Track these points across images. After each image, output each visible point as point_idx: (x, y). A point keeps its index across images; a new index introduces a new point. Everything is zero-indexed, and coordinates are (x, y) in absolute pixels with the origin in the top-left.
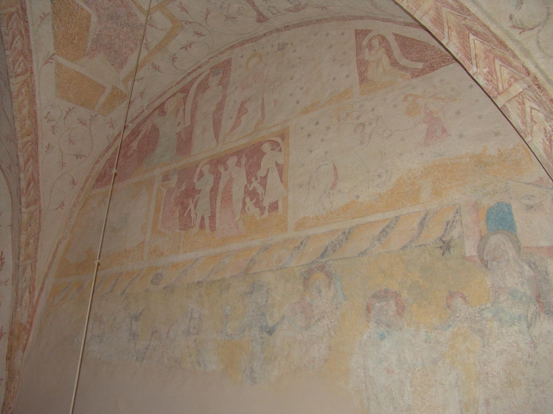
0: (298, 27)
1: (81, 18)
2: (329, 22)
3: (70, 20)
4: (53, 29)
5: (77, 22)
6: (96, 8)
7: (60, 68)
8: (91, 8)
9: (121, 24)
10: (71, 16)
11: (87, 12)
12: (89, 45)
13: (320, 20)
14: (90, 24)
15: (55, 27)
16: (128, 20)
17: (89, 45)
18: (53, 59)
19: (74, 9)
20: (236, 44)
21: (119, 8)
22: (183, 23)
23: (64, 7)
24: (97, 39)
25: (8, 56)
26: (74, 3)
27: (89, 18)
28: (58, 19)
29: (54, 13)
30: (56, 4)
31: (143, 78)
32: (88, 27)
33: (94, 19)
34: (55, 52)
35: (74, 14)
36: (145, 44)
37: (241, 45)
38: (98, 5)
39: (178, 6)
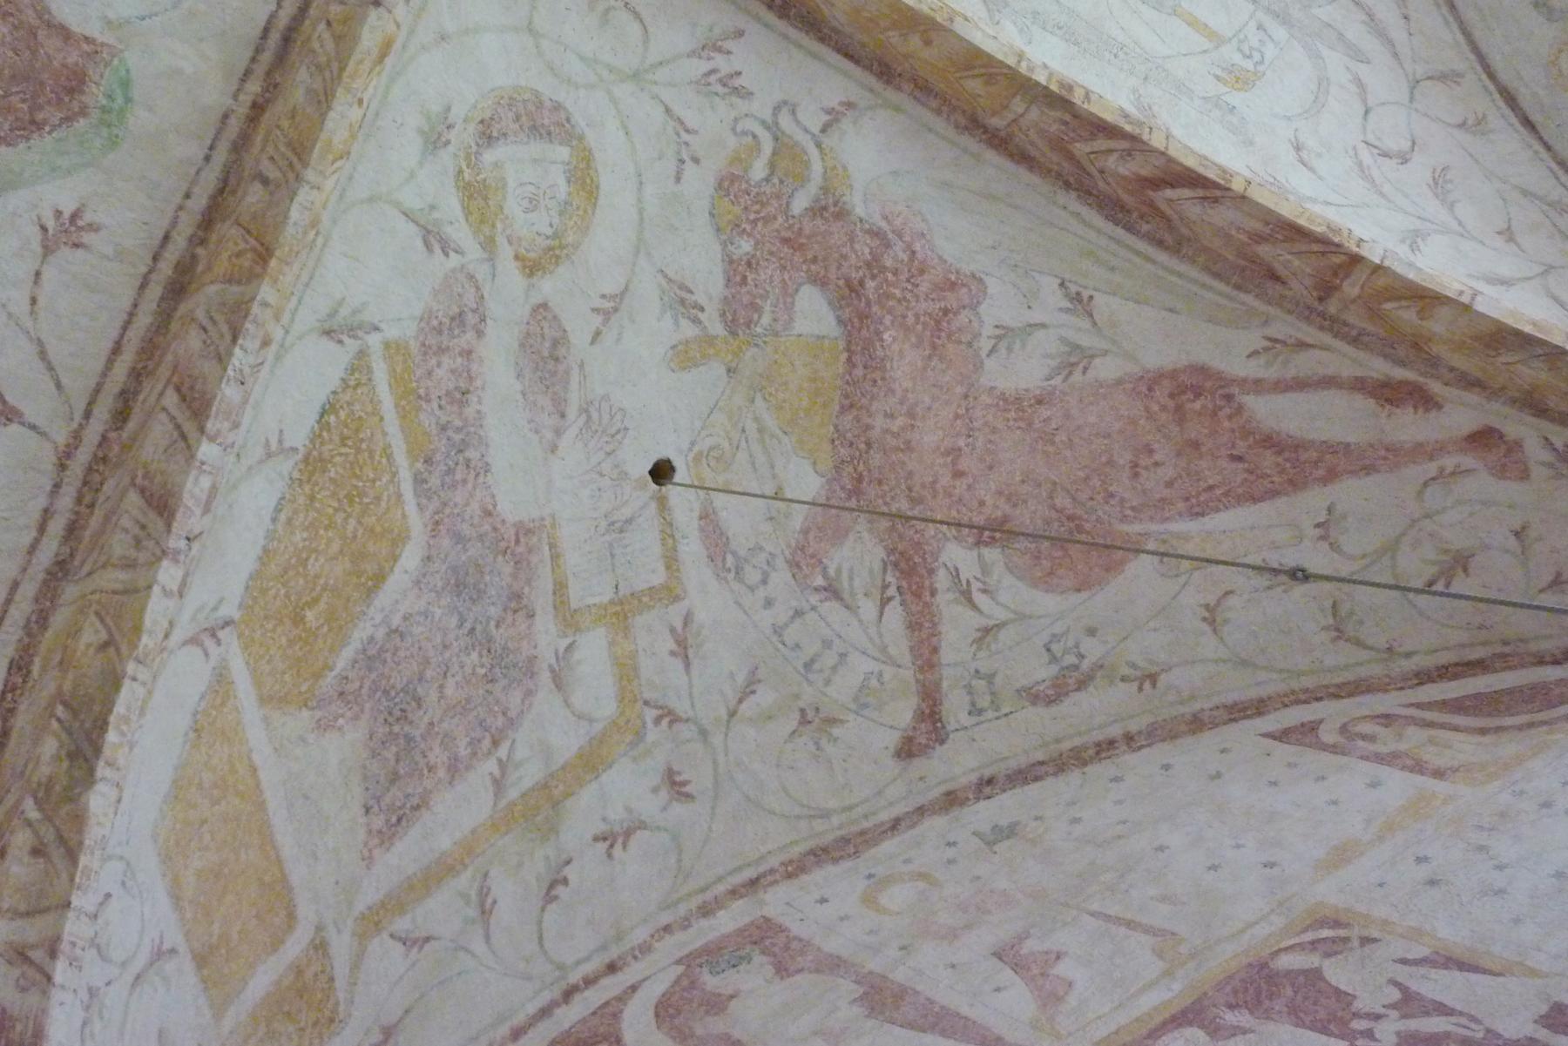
0: (1026, 782)
1: (378, 529)
2: (1140, 748)
3: (339, 518)
4: (274, 520)
5: (355, 537)
6: (437, 517)
7: (219, 701)
8: (420, 507)
9: (472, 630)
10: (351, 502)
11: (404, 516)
12: (343, 660)
13: (1111, 743)
14: (392, 569)
15: (283, 517)
16: (497, 626)
17: (343, 660)
18: (219, 643)
19: (374, 481)
20: (772, 871)
21: (500, 558)
22: (650, 714)
23: (347, 455)
24: (382, 650)
25: (203, 463)
26: (384, 460)
27: (399, 540)
28: (307, 488)
29: (306, 460)
30: (329, 431)
31: (427, 939)
32: (380, 578)
33: (410, 558)
34: (236, 615)
35: (366, 500)
36: (500, 761)
37: (789, 876)
38: (447, 511)
39: (673, 630)
